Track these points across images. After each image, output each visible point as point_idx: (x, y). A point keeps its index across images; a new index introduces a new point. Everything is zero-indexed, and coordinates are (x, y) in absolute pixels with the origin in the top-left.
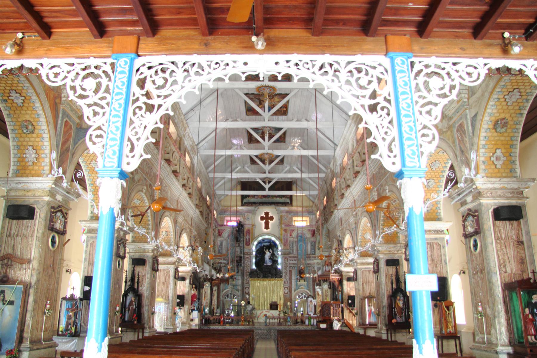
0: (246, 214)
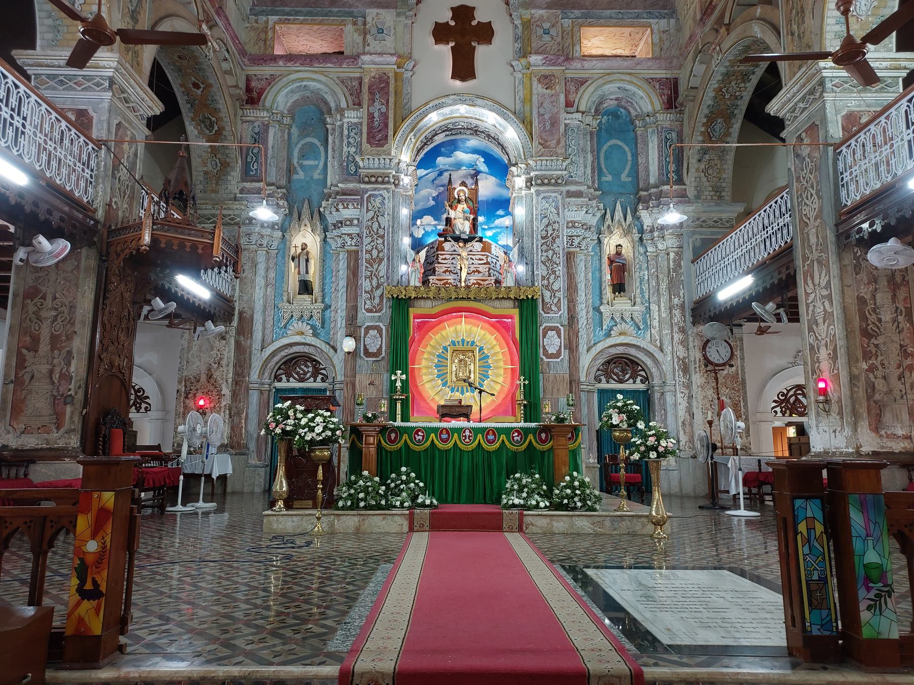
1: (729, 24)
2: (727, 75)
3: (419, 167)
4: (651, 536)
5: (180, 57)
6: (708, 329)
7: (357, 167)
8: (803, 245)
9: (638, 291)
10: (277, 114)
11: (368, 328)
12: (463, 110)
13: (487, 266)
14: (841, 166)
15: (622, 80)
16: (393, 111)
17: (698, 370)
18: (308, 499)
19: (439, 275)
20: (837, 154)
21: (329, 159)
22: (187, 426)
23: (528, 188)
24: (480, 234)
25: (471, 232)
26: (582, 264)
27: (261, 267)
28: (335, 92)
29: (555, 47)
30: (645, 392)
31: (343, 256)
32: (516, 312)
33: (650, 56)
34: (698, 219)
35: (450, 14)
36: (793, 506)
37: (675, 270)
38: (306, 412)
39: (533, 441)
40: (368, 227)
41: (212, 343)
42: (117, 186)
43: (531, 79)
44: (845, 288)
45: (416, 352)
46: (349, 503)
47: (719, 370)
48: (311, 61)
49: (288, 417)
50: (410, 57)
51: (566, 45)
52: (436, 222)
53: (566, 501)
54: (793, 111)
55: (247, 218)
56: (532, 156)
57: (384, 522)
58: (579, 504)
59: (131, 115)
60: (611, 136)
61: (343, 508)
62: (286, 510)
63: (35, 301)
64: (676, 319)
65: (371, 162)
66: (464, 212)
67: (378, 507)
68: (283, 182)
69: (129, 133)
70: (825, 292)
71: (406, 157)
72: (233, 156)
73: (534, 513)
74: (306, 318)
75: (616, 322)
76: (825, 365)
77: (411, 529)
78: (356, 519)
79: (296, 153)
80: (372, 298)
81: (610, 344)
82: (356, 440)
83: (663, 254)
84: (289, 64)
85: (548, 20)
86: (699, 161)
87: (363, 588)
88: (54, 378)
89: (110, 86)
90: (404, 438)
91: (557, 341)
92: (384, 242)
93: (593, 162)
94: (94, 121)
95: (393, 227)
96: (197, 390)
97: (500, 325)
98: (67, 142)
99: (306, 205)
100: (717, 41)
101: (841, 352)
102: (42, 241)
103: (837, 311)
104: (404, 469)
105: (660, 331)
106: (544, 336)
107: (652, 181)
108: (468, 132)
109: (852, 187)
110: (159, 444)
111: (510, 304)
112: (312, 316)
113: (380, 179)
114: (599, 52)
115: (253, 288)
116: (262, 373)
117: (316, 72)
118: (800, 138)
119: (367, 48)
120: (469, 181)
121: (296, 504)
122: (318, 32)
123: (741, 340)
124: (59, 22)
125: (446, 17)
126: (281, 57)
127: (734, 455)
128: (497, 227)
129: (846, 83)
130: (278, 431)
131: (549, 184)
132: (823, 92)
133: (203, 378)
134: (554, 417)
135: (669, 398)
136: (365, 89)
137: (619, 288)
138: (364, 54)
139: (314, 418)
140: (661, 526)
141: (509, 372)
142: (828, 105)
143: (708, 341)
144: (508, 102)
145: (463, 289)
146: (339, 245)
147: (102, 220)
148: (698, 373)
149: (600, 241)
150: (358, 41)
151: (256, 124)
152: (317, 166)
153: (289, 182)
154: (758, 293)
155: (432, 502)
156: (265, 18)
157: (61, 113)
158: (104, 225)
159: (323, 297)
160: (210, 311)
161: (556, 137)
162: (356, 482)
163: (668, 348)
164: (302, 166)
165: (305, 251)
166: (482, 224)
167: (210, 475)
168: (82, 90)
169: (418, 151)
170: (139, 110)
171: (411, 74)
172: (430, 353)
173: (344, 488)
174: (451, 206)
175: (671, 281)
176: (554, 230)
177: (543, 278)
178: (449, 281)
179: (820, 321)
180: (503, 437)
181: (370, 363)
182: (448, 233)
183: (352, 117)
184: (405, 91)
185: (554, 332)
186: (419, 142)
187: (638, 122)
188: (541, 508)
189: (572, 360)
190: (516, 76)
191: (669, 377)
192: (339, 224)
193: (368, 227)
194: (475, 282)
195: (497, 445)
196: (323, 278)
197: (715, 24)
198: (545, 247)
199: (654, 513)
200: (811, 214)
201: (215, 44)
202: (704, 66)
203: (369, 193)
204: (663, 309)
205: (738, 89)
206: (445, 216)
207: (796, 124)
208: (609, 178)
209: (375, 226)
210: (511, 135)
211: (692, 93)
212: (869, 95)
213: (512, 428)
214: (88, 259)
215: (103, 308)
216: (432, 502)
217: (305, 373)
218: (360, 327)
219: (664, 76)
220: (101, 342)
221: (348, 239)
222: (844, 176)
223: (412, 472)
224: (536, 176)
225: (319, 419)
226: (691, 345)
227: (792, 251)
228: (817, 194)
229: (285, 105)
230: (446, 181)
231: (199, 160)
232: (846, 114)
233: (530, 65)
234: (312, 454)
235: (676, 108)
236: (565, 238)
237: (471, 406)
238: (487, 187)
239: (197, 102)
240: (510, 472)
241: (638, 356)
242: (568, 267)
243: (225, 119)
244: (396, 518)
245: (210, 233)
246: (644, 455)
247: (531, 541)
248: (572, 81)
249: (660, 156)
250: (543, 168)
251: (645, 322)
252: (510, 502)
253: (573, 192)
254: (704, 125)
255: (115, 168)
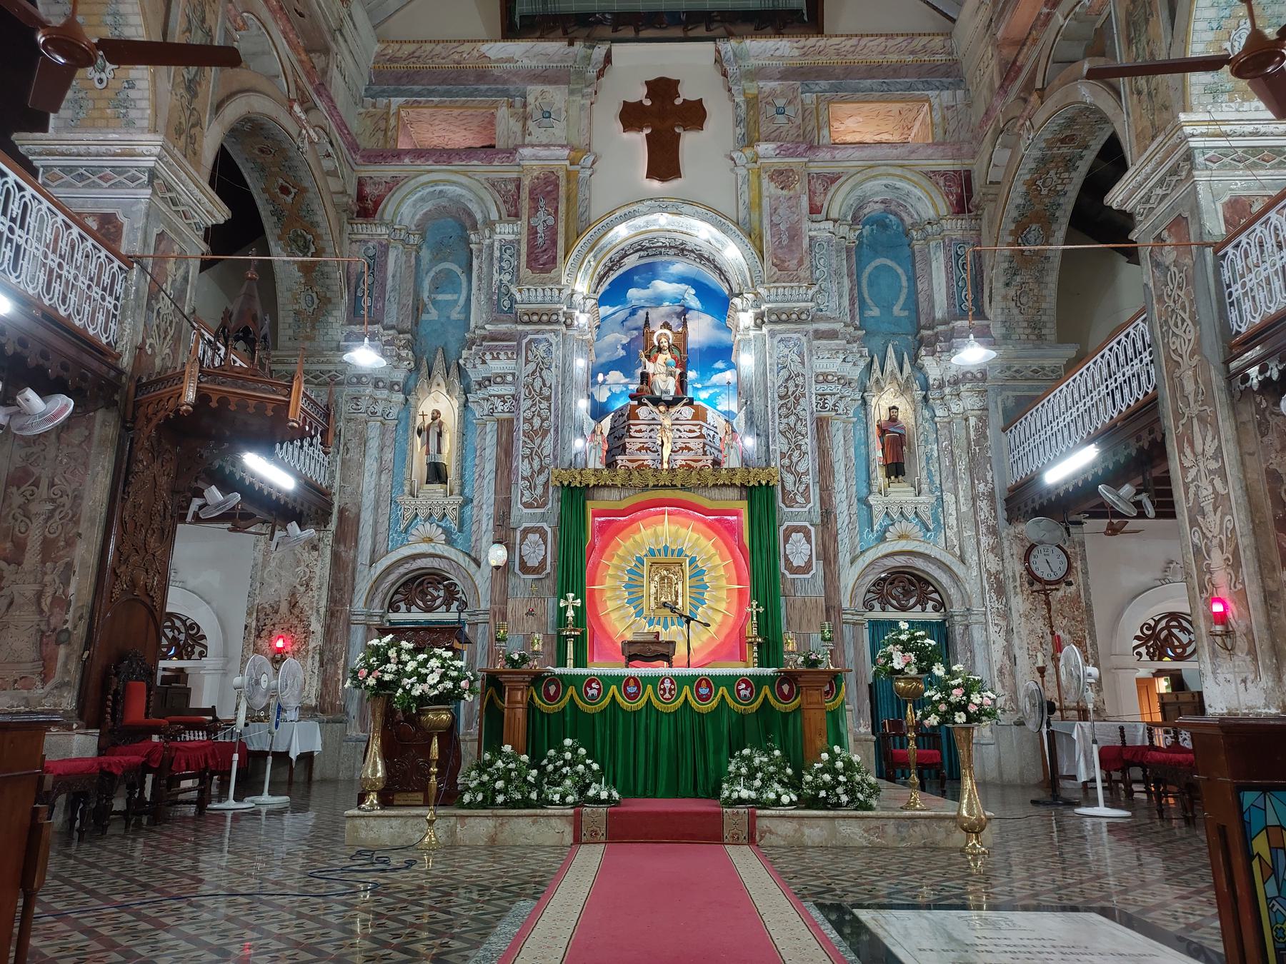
0: (534, 91)
1: (1043, 89)
2: (1043, 162)
3: (602, 301)
4: (962, 850)
5: (261, 151)
6: (1033, 528)
7: (513, 301)
8: (1174, 397)
9: (924, 473)
10: (400, 230)
11: (526, 532)
12: (663, 220)
13: (701, 440)
14: (1226, 275)
15: (889, 175)
16: (563, 224)
17: (1018, 590)
18: (416, 791)
19: (631, 454)
20: (1220, 258)
21: (473, 292)
22: (246, 678)
23: (758, 327)
24: (690, 395)
25: (677, 392)
26: (840, 436)
27: (374, 445)
28: (482, 199)
29: (793, 131)
30: (941, 625)
31: (491, 427)
32: (743, 506)
33: (930, 141)
34: (1009, 368)
35: (645, 91)
36: (1241, 805)
37: (977, 443)
38: (414, 653)
39: (770, 696)
40: (527, 386)
41: (299, 555)
42: (155, 322)
43: (759, 176)
44: (1247, 457)
45: (596, 566)
46: (480, 797)
47: (1052, 590)
48: (449, 158)
49: (388, 661)
50: (588, 149)
51: (809, 128)
52: (627, 380)
53: (823, 794)
54: (1148, 201)
55: (354, 376)
56: (763, 282)
57: (534, 829)
58: (844, 798)
59: (180, 223)
60: (877, 254)
61: (471, 805)
62: (382, 809)
63: (23, 489)
64: (982, 513)
65: (533, 293)
66: (667, 364)
67: (527, 804)
68: (408, 324)
69: (176, 247)
70: (1214, 465)
71: (582, 286)
72: (336, 288)
73: (773, 812)
74: (436, 517)
75: (892, 519)
76: (1221, 577)
77: (577, 840)
78: (490, 823)
79: (426, 284)
80: (532, 487)
81: (884, 552)
82: (495, 696)
83: (958, 419)
84: (418, 162)
85: (783, 95)
86: (1007, 285)
87: (476, 945)
88: (43, 604)
89: (151, 182)
90: (569, 693)
91: (805, 548)
92: (550, 406)
93: (851, 290)
94: (125, 229)
95: (563, 385)
96: (274, 625)
97: (721, 526)
98: (78, 256)
99: (439, 356)
100: (1025, 114)
101: (1247, 556)
102: (31, 398)
103: (1234, 491)
104: (568, 742)
105: (960, 532)
106: (786, 541)
107: (939, 314)
108: (672, 252)
109: (1247, 305)
110: (214, 707)
111: (734, 493)
112: (445, 515)
113: (545, 318)
114: (857, 138)
115: (361, 474)
116: (370, 600)
117: (457, 172)
118: (1159, 238)
119: (528, 139)
120: (674, 322)
121: (398, 798)
122: (460, 118)
123: (1082, 544)
124: (82, 94)
125: (639, 94)
126: (408, 152)
127: (1080, 720)
128: (714, 386)
129: (1226, 156)
130: (371, 681)
131: (788, 321)
132: (1191, 169)
133: (284, 607)
134: (801, 659)
135: (977, 633)
136: (525, 194)
137: (896, 469)
138: (524, 146)
139: (426, 661)
140: (977, 833)
141: (735, 594)
142: (1200, 188)
143: (1033, 546)
144: (727, 207)
145: (664, 473)
146: (485, 413)
147: (129, 370)
148: (1020, 596)
149: (864, 402)
150: (515, 129)
151: (370, 244)
152: (456, 302)
153: (417, 324)
154: (1106, 469)
155: (610, 795)
156: (385, 101)
157: (78, 219)
158: (132, 377)
159: (462, 486)
160: (294, 508)
161: (798, 255)
162: (491, 763)
163: (972, 559)
164: (434, 302)
165: (437, 421)
166: (693, 381)
167: (287, 753)
168: (110, 187)
169: (601, 279)
170: (194, 217)
171: (589, 172)
172: (617, 567)
173: (473, 773)
174: (648, 357)
175: (972, 459)
176: (797, 386)
177: (783, 455)
178: (645, 463)
179: (1209, 508)
180: (723, 690)
181: (529, 582)
182: (645, 395)
183: (506, 232)
184: (580, 196)
185: (801, 535)
186: (600, 267)
187: (915, 233)
188: (784, 805)
189: (829, 576)
190: (739, 172)
191: (976, 600)
192: (487, 382)
193: (527, 386)
194: (684, 463)
195: (713, 703)
196: (462, 459)
197: (1022, 91)
198: (784, 411)
199: (965, 813)
200: (1184, 348)
201: (312, 132)
202: (1008, 153)
203: (530, 337)
204: (962, 500)
205: (1060, 181)
206: (639, 371)
207: (1152, 218)
208: (876, 312)
209: (538, 384)
210: (733, 253)
211: (993, 190)
212: (1263, 172)
213: (737, 677)
214: (104, 425)
215: (123, 498)
216: (610, 795)
217: (434, 599)
218: (514, 529)
219: (950, 168)
220: (117, 548)
221: (498, 403)
222: (1233, 289)
223: (580, 746)
224: (770, 309)
225: (434, 663)
226: (1007, 553)
227: (1156, 406)
228: (1192, 318)
229: (413, 218)
230: (641, 323)
231: (289, 295)
232: (1230, 201)
233: (758, 157)
234: (422, 718)
235: (970, 211)
236: (814, 397)
237: (673, 643)
238: (700, 330)
239: (286, 213)
240: (735, 746)
241: (928, 569)
242: (819, 440)
243: (325, 238)
244: (553, 821)
245: (285, 387)
246: (946, 718)
247: (768, 861)
248: (818, 178)
249: (949, 279)
250: (779, 298)
251: (936, 520)
252: (735, 795)
253: (823, 332)
254: (1012, 233)
255: (153, 296)
